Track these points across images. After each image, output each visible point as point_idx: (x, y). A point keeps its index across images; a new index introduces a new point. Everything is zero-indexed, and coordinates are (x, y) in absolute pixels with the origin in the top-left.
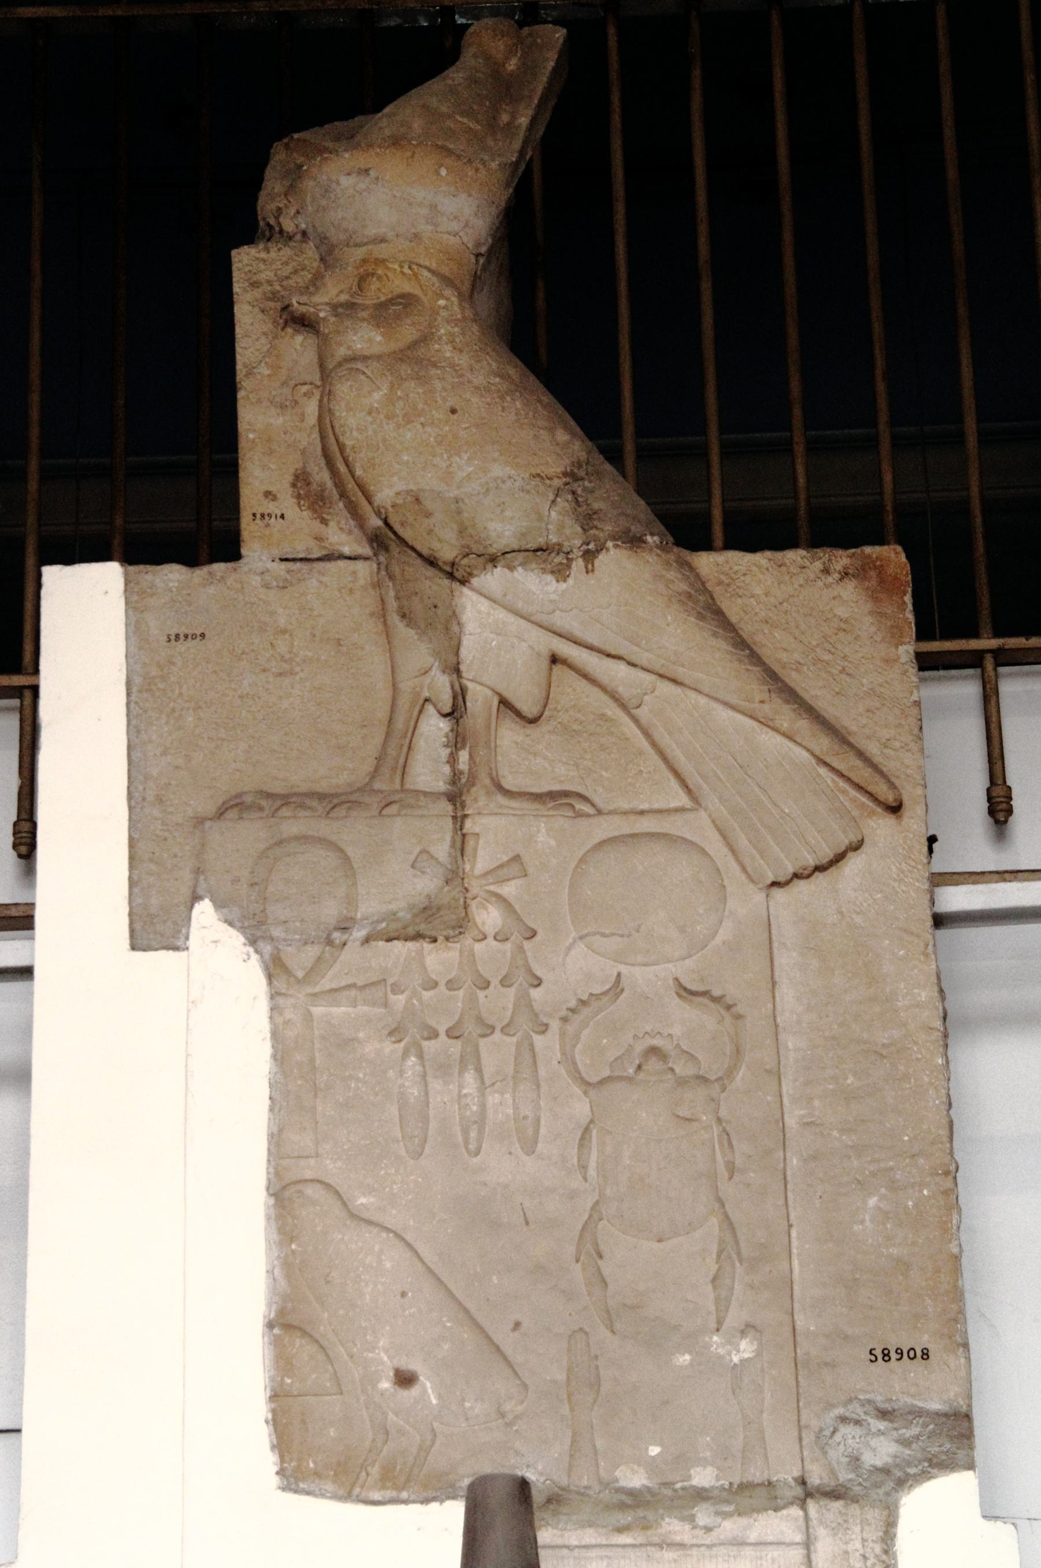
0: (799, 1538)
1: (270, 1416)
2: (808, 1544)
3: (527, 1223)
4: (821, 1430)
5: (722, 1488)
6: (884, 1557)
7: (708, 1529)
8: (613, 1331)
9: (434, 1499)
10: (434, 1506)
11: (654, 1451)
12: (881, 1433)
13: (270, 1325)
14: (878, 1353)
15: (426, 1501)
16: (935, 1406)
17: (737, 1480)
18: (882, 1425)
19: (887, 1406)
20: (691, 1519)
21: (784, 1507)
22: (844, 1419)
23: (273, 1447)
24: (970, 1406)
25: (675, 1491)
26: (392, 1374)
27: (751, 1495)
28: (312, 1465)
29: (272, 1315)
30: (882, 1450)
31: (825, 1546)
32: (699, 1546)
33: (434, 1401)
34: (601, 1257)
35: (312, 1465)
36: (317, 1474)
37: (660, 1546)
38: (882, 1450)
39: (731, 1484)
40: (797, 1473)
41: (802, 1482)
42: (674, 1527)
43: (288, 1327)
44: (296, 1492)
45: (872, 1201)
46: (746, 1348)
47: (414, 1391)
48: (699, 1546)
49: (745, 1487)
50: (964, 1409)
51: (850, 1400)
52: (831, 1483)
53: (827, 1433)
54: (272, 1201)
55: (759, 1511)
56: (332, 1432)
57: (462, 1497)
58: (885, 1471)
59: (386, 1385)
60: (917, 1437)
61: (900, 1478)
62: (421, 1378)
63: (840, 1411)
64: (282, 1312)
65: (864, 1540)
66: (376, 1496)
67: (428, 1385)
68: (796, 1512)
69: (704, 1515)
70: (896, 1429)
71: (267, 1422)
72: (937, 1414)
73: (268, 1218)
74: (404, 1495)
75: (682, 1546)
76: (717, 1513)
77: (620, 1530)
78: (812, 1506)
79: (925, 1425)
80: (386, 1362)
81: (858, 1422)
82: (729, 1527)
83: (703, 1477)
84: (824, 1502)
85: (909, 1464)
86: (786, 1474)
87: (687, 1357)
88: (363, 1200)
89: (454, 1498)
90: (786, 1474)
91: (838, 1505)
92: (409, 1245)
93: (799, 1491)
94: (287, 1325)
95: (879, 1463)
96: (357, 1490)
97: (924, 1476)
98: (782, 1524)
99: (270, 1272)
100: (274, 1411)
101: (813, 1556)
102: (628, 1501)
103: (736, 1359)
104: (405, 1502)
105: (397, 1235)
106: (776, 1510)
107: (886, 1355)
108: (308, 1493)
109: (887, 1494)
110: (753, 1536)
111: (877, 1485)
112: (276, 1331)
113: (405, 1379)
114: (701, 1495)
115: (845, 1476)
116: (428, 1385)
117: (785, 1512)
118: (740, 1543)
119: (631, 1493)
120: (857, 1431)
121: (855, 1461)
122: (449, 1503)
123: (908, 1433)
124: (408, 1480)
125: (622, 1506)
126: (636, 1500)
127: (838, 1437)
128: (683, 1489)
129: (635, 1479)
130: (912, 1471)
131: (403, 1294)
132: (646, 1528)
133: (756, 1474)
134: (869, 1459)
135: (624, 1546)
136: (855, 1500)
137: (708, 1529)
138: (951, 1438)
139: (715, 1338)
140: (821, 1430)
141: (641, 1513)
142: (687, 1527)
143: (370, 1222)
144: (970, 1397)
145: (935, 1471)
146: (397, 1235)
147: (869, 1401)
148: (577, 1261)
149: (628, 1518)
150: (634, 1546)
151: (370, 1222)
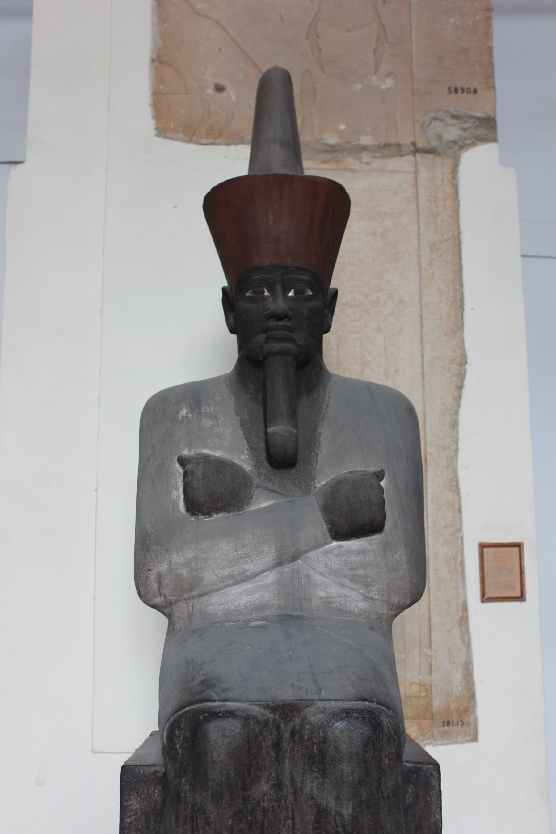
0: (412, 169)
1: (152, 103)
2: (416, 173)
3: (282, 20)
4: (424, 123)
5: (375, 146)
6: (452, 181)
7: (368, 164)
8: (324, 72)
9: (233, 144)
10: (233, 147)
11: (342, 127)
12: (452, 125)
13: (153, 61)
14: (453, 89)
15: (229, 144)
16: (479, 114)
17: (382, 142)
18: (453, 122)
19: (455, 113)
20: (360, 159)
21: (405, 155)
22: (435, 119)
23: (153, 117)
24: (495, 115)
25: (352, 146)
26: (213, 86)
27: (389, 149)
28: (172, 126)
29: (154, 56)
30: (453, 132)
31: (424, 175)
32: (363, 171)
33: (234, 99)
34: (318, 37)
35: (172, 126)
36: (175, 131)
37: (344, 170)
38: (453, 132)
39: (380, 144)
40: (412, 140)
41: (414, 144)
42: (350, 161)
43: (161, 62)
44: (165, 137)
45: (452, 21)
46: (389, 83)
47: (224, 94)
48: (363, 171)
49: (386, 145)
50: (493, 116)
51: (438, 110)
52: (427, 146)
53: (427, 124)
54: (155, 4)
55: (391, 156)
56: (183, 111)
57: (248, 144)
58: (454, 142)
59: (210, 91)
60: (470, 128)
61: (462, 145)
62: (228, 89)
63: (433, 115)
64: (159, 56)
65: (443, 173)
66: (204, 141)
67: (231, 92)
68: (411, 157)
69: (366, 157)
70: (460, 124)
71: (150, 105)
72: (479, 119)
73: (153, 11)
74: (218, 141)
75: (354, 171)
76: (373, 157)
77: (325, 162)
78: (418, 155)
79: (474, 123)
80: (210, 80)
81: (441, 120)
82: (378, 163)
83: (366, 140)
84: (424, 155)
85: (465, 139)
86: (407, 141)
87: (359, 86)
88: (200, 6)
89: (243, 143)
90: (407, 141)
91: (431, 156)
92: (223, 28)
93: (413, 149)
94: (161, 62)
95: (451, 139)
96: (194, 138)
97: (473, 145)
98: (405, 163)
99: (153, 36)
100: (154, 100)
101: (418, 179)
102: (329, 149)
103: (384, 87)
104: (218, 144)
105: (218, 23)
106: (402, 156)
107: (456, 91)
108: (170, 138)
109: (455, 152)
110: (390, 167)
111: (450, 148)
112: (156, 63)
113: (220, 89)
114: (364, 148)
115: (434, 144)
116: (231, 92)
117: (405, 158)
118: (383, 171)
119: (331, 146)
120: (441, 124)
121: (439, 137)
122: (240, 147)
123: (466, 126)
124: (220, 134)
125: (326, 151)
126: (333, 149)
127: (432, 126)
128: (357, 145)
129: (332, 140)
130: (467, 142)
131: (220, 50)
132: (337, 161)
133: (392, 140)
134: (447, 137)
135: (326, 169)
136: (439, 154)
137: (368, 164)
138: (486, 128)
139: (374, 78)
140: (424, 123)
141: (335, 154)
142: (358, 162)
143: (204, 16)
144: (494, 111)
145: (478, 143)
146: (218, 23)
147: (447, 111)
148: (307, 38)
149: (329, 156)
150: (331, 170)
151: (204, 16)
